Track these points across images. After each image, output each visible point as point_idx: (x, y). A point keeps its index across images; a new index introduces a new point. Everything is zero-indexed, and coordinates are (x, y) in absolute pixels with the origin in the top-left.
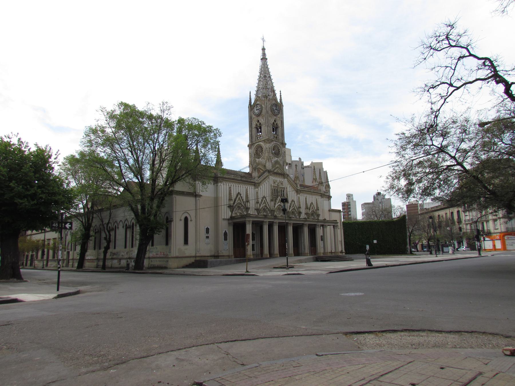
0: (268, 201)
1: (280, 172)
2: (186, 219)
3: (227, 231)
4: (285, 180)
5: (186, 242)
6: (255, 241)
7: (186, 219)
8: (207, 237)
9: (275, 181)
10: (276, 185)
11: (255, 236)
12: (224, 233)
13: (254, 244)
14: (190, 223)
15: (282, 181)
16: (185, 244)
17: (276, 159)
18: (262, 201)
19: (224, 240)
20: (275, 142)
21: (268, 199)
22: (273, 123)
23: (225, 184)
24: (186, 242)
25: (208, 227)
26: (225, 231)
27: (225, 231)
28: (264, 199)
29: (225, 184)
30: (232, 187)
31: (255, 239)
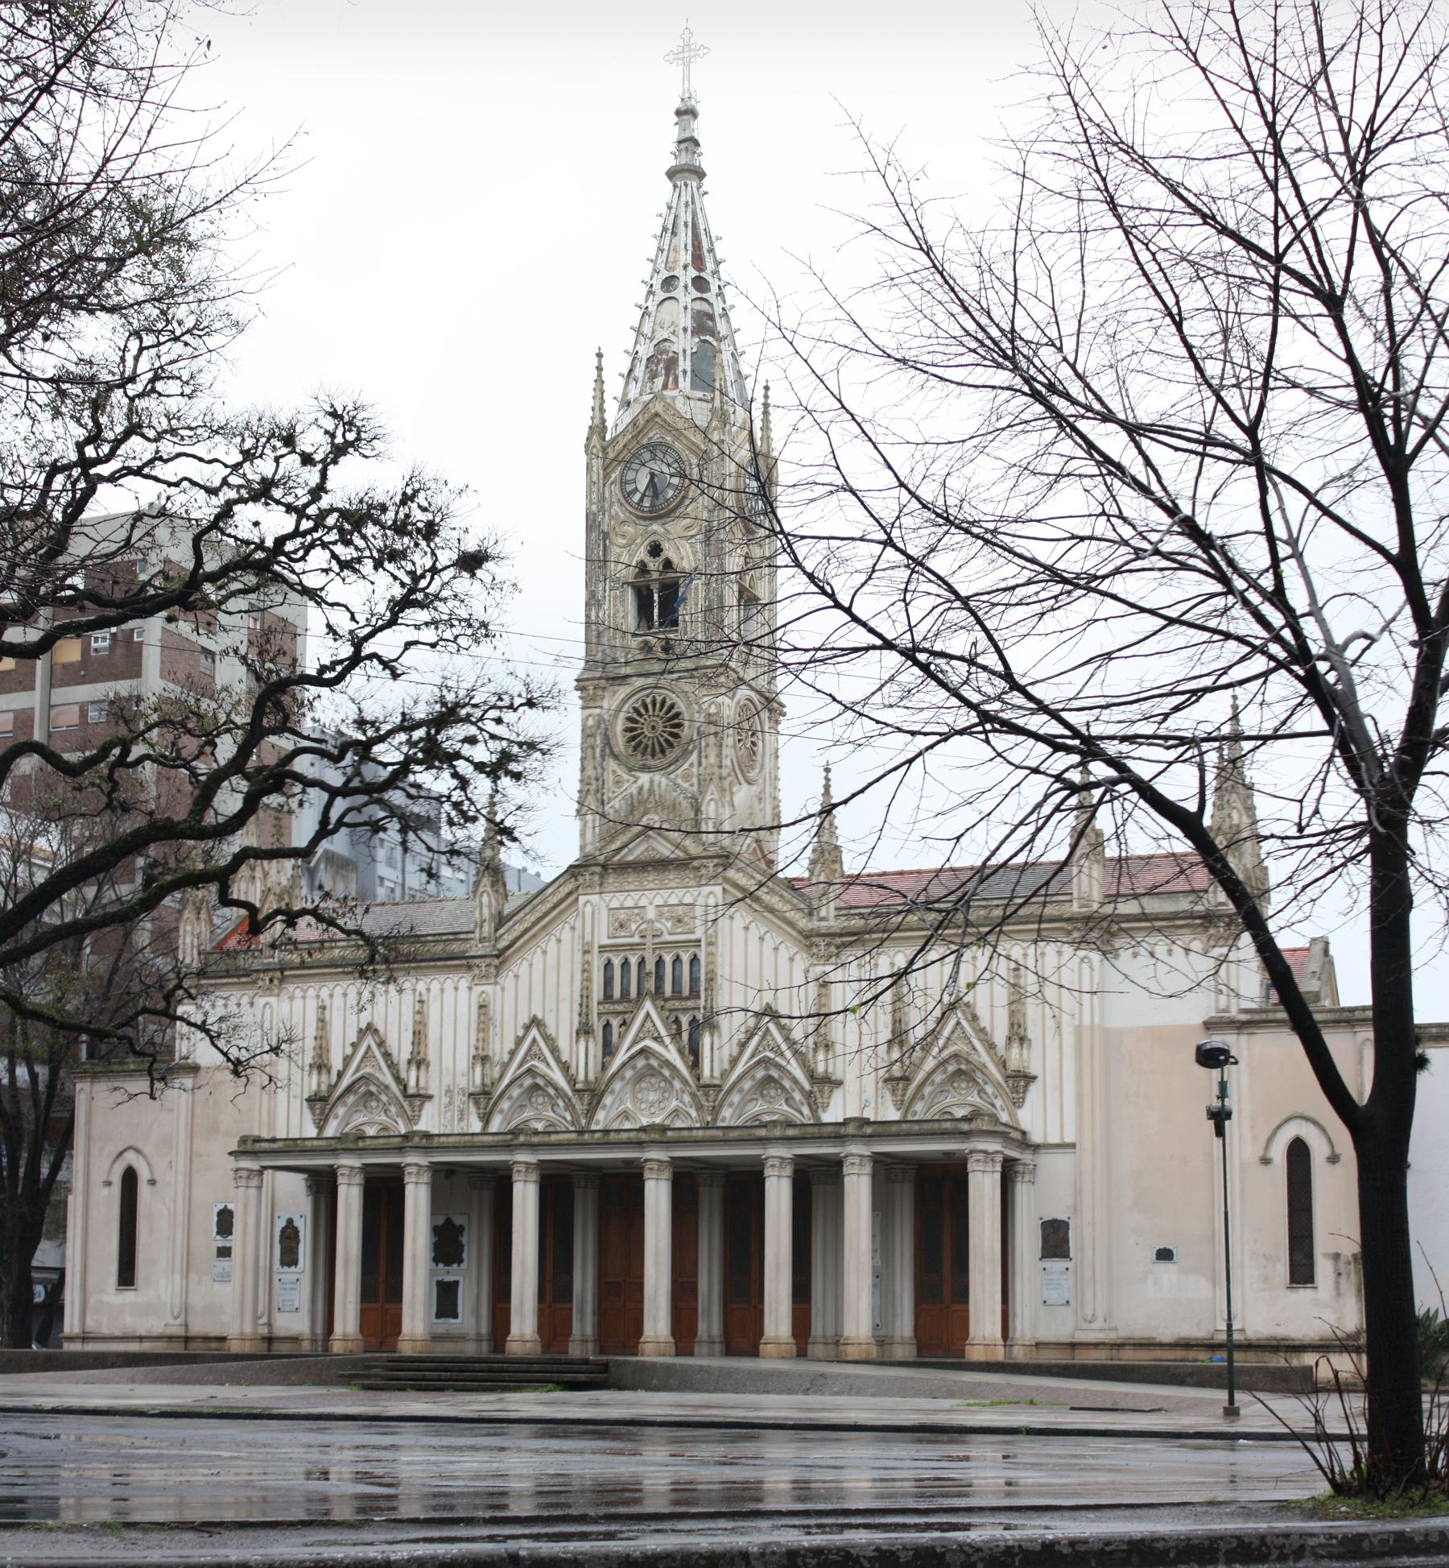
0: (564, 1042)
1: (667, 853)
2: (130, 1179)
3: (299, 1223)
4: (706, 890)
5: (127, 1275)
6: (464, 1266)
7: (130, 1179)
8: (224, 1252)
9: (622, 915)
10: (636, 939)
11: (464, 1239)
12: (284, 1230)
13: (456, 1283)
14: (144, 1192)
15: (688, 899)
16: (120, 1284)
17: (644, 778)
18: (519, 1041)
19: (283, 1263)
20: (639, 682)
21: (563, 1028)
22: (643, 568)
23: (299, 993)
24: (127, 1275)
25: (230, 1206)
26: (290, 1222)
27: (290, 1222)
28: (534, 1032)
29: (299, 993)
30: (338, 1000)
31: (465, 1255)
